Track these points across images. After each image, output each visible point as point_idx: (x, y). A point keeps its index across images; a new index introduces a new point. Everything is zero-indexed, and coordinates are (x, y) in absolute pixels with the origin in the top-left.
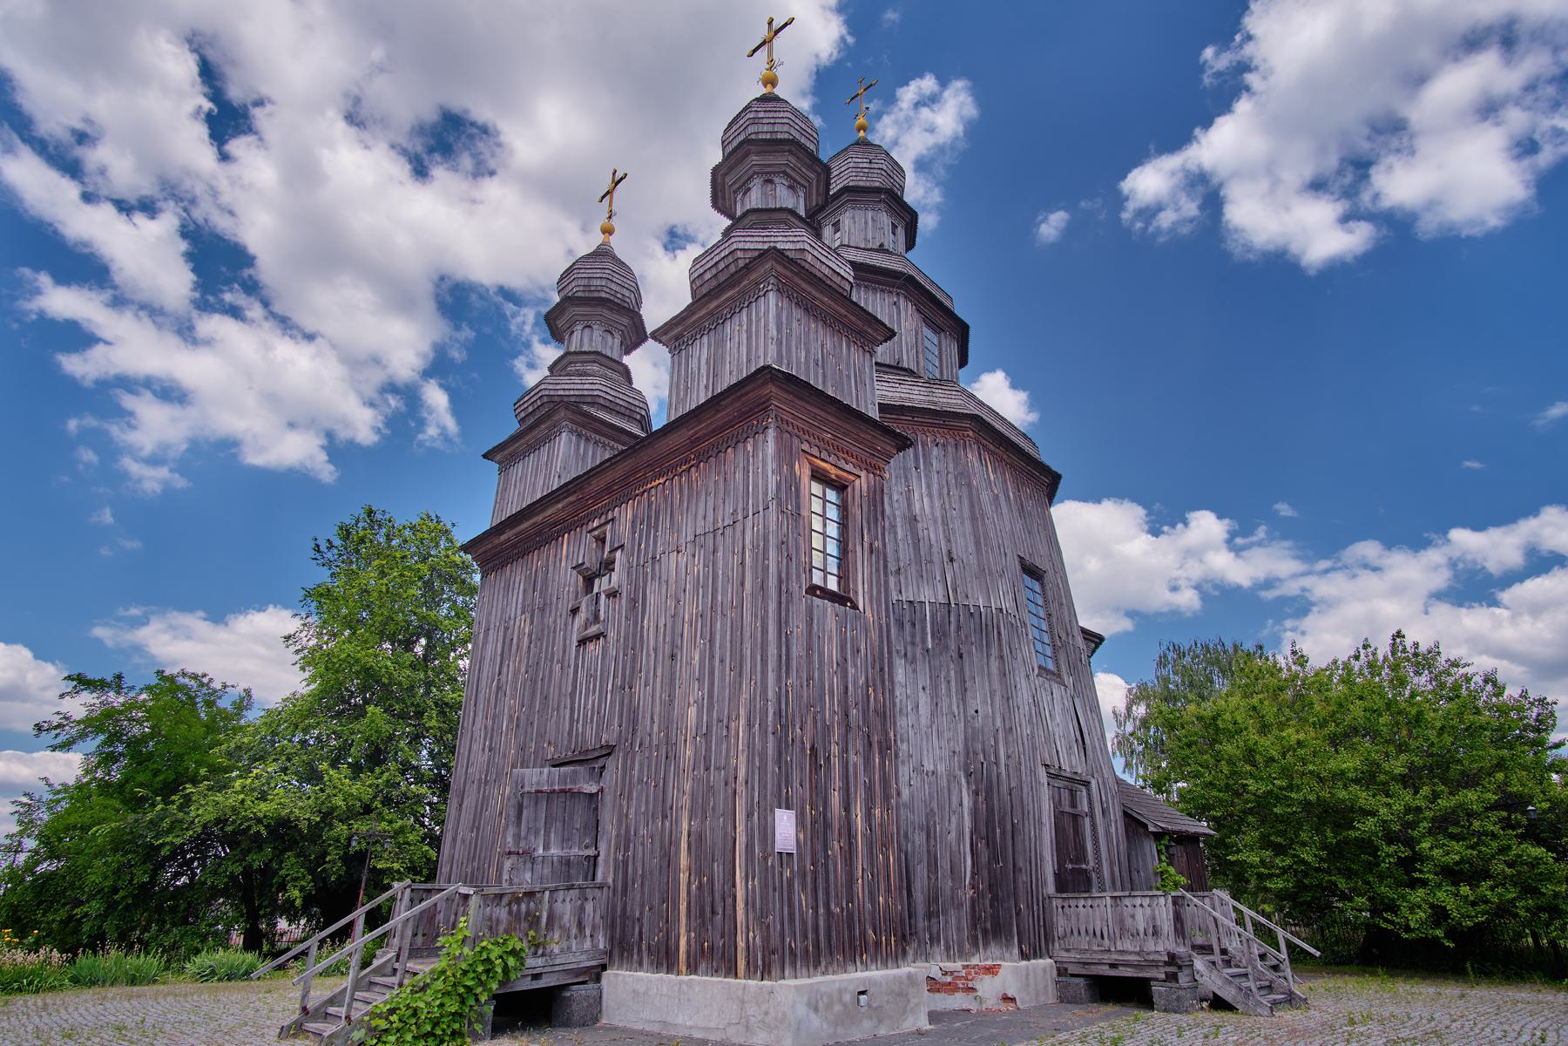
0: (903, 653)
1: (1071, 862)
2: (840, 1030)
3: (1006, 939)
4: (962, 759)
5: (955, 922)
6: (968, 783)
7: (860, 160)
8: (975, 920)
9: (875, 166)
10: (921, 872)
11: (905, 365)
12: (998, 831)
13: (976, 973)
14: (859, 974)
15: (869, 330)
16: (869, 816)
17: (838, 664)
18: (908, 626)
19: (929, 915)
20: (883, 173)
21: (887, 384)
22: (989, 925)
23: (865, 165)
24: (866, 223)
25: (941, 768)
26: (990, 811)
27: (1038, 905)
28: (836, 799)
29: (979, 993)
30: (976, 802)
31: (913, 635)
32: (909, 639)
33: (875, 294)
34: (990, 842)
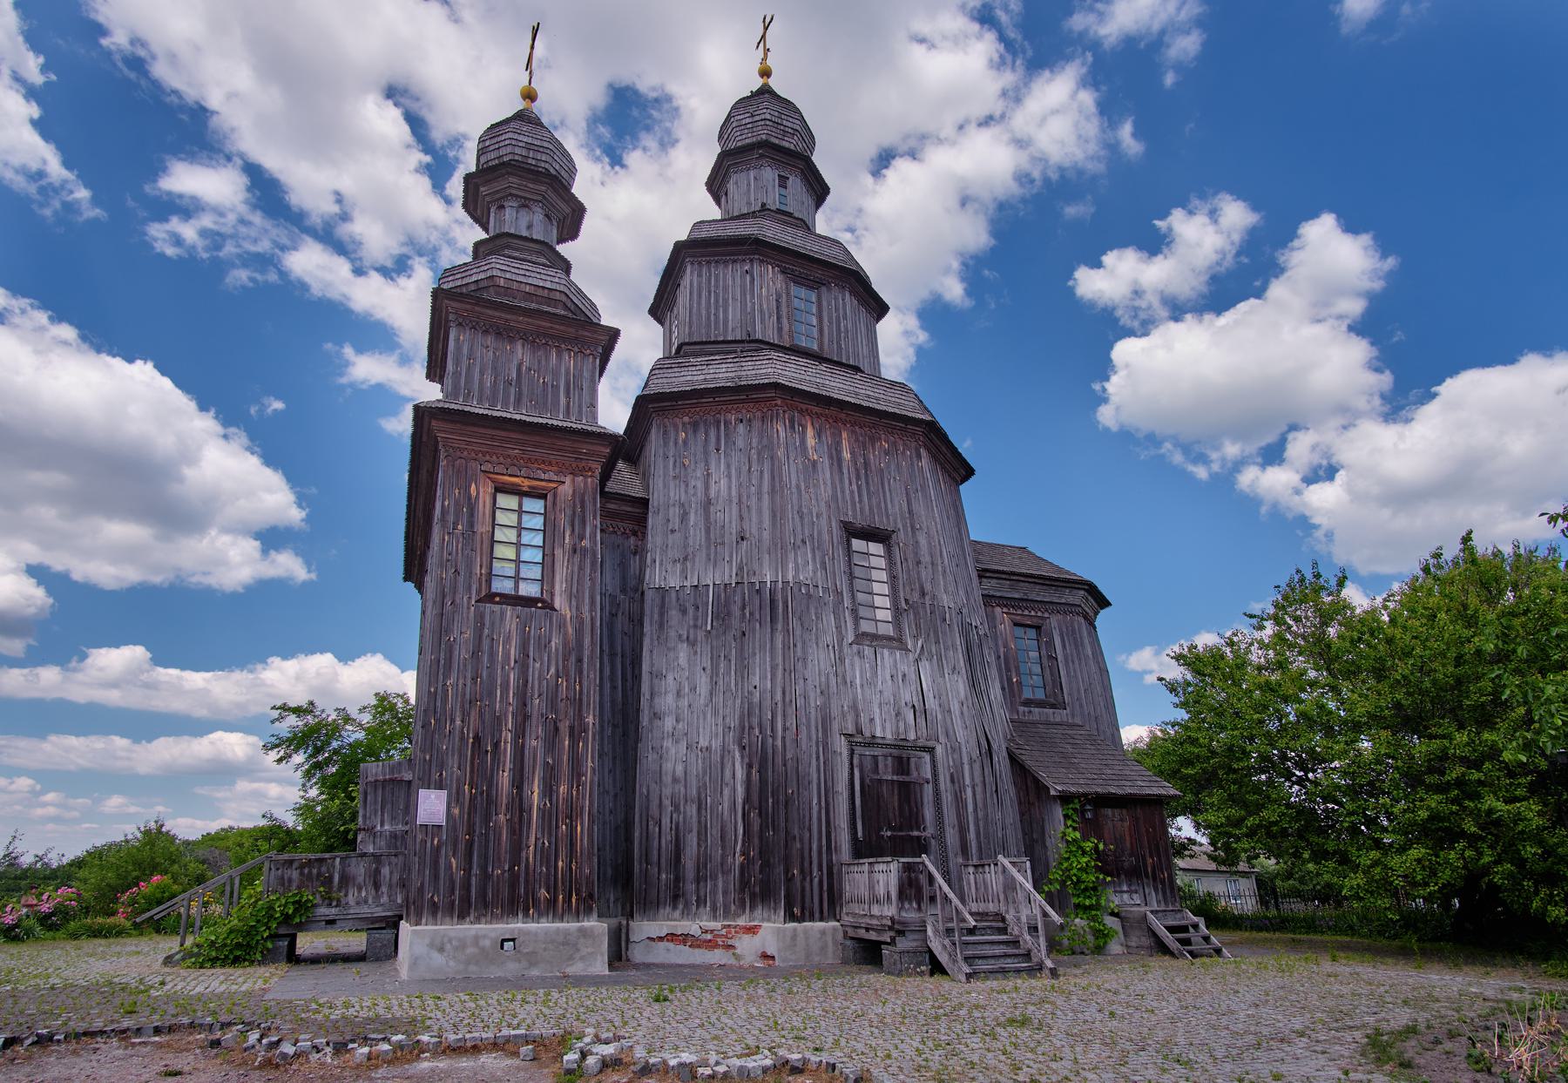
0: (685, 636)
1: (890, 828)
2: (472, 968)
3: (775, 903)
4: (737, 735)
5: (724, 886)
6: (742, 757)
7: (742, 117)
8: (744, 883)
9: (757, 118)
10: (692, 841)
11: (759, 336)
12: (770, 801)
13: (736, 932)
14: (520, 925)
15: (586, 334)
17: (516, 662)
18: (691, 611)
19: (698, 880)
20: (768, 123)
21: (694, 368)
22: (757, 889)
23: (748, 120)
24: (749, 185)
25: (716, 744)
26: (763, 781)
27: (820, 869)
28: (505, 779)
29: (738, 951)
30: (749, 775)
31: (696, 619)
32: (691, 623)
33: (726, 267)
34: (762, 813)
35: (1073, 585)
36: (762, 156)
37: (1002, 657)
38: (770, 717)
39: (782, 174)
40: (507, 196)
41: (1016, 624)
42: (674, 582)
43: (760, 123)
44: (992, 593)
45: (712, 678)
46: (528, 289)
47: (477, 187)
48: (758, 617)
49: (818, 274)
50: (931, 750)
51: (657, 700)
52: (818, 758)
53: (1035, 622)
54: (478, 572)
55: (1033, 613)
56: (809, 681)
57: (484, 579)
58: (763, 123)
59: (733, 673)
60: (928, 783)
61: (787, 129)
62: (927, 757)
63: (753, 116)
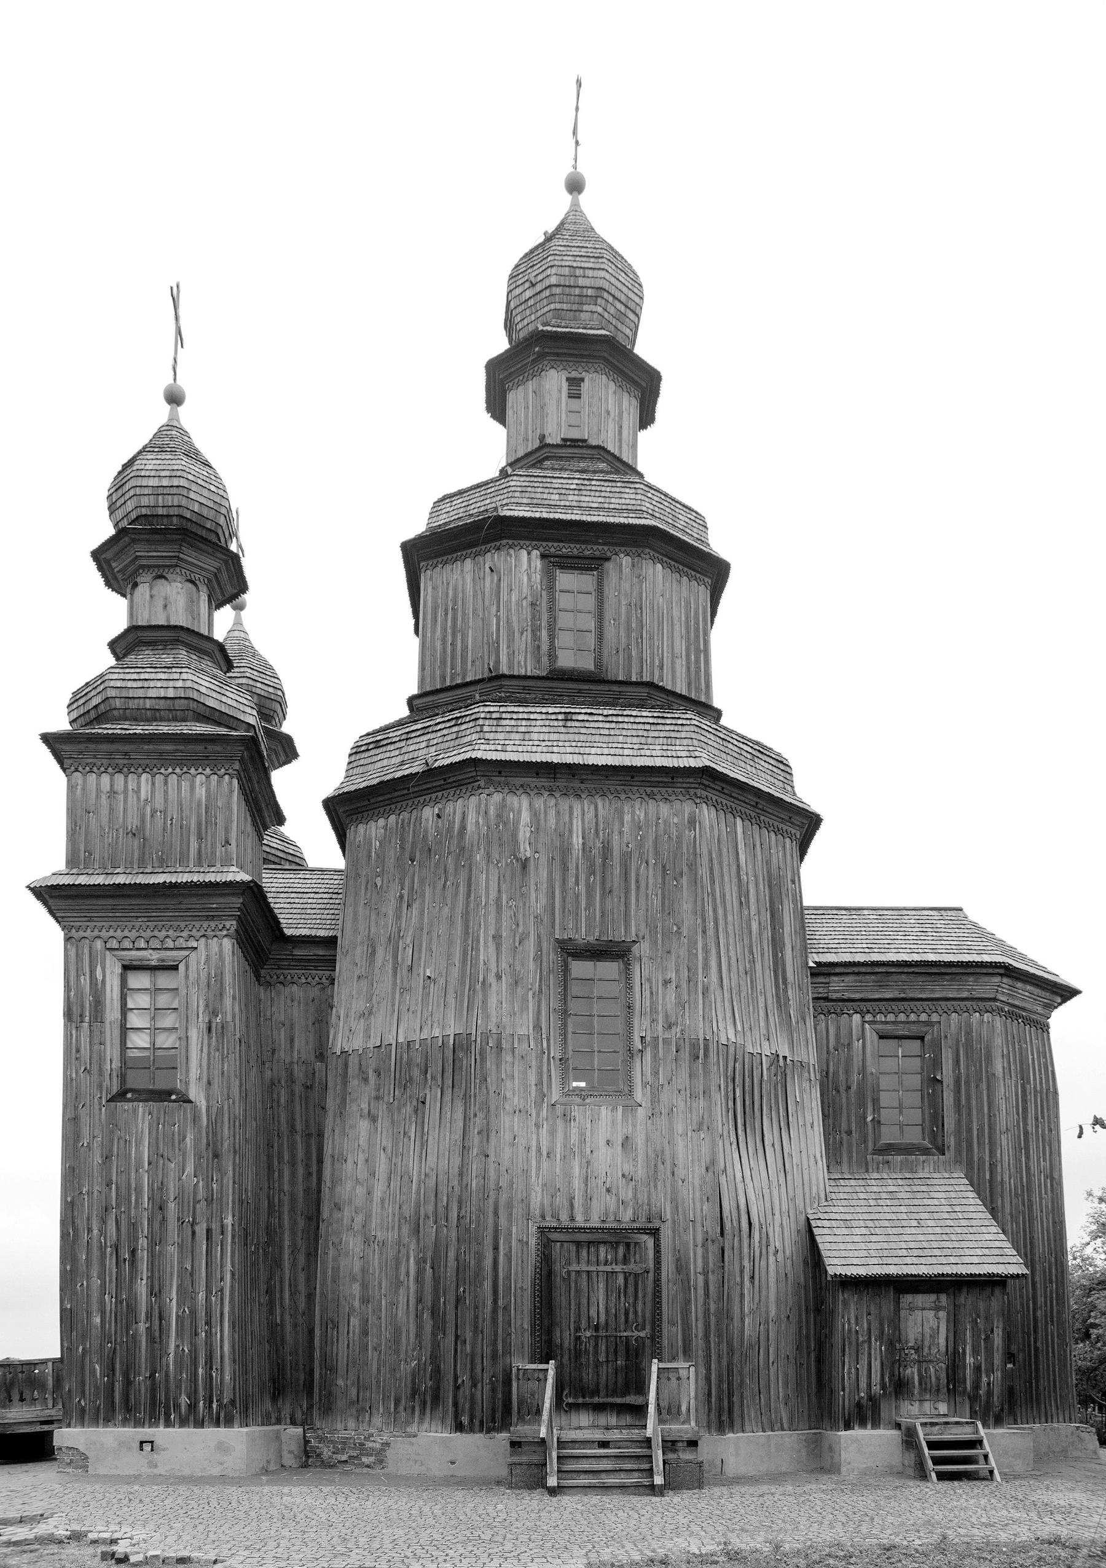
9: (539, 288)
16: (186, 1294)
18: (372, 1077)
21: (392, 747)
23: (528, 294)
35: (978, 970)
36: (541, 356)
37: (854, 1087)
38: (445, 1203)
40: (137, 570)
41: (881, 1037)
42: (357, 1043)
43: (544, 295)
44: (847, 995)
45: (390, 1160)
47: (108, 562)
48: (440, 1083)
49: (595, 550)
50: (655, 1233)
51: (338, 1189)
52: (496, 1248)
53: (915, 1030)
54: (109, 1068)
55: (913, 1017)
56: (492, 1158)
57: (115, 1074)
58: (547, 293)
59: (412, 1153)
60: (648, 1272)
62: (650, 1242)
63: (533, 285)
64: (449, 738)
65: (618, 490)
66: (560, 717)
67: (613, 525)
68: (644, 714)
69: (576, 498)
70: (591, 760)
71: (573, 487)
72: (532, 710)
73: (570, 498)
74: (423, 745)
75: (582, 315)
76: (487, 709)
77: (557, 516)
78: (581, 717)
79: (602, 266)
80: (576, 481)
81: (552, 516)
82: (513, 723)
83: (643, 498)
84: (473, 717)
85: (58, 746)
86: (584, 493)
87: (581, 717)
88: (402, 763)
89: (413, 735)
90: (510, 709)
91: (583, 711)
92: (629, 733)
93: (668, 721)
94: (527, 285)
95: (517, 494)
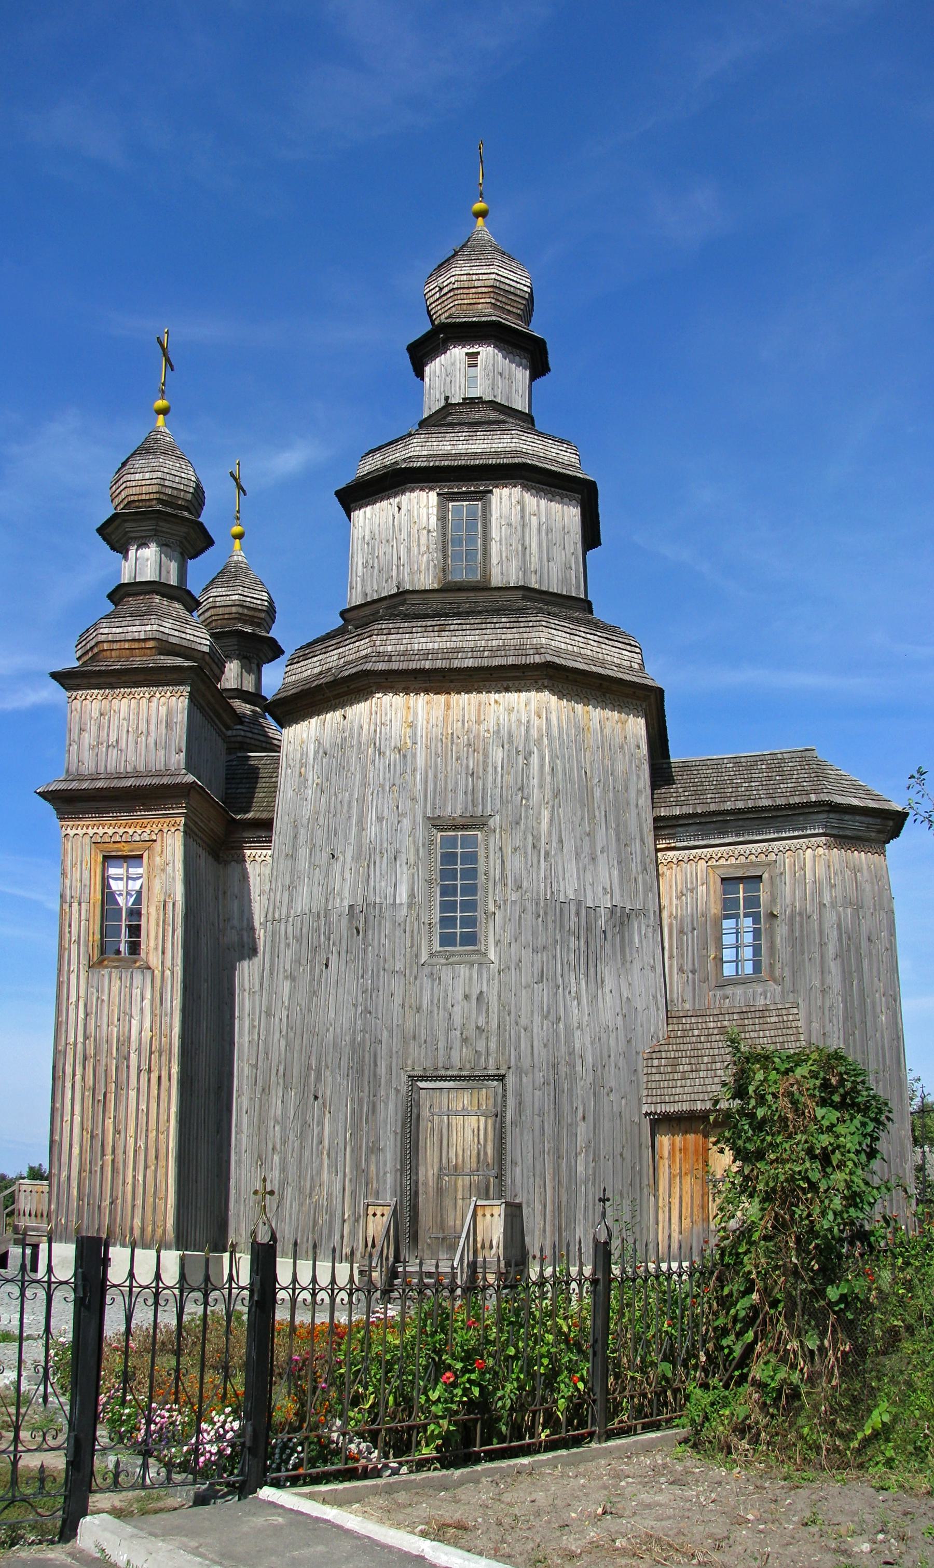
21: (315, 659)
39: (472, 350)
46: (127, 645)
58: (452, 294)
61: (480, 290)
64: (353, 651)
65: (498, 437)
66: (436, 628)
67: (491, 465)
68: (503, 620)
69: (464, 447)
70: (456, 664)
71: (462, 438)
72: (414, 624)
73: (460, 447)
74: (336, 657)
75: (480, 306)
76: (380, 627)
77: (446, 463)
78: (452, 627)
79: (492, 271)
80: (464, 434)
81: (443, 463)
82: (399, 636)
83: (517, 441)
84: (369, 634)
85: (62, 681)
86: (471, 442)
87: (452, 627)
88: (321, 673)
89: (330, 648)
90: (398, 625)
91: (455, 622)
92: (490, 637)
93: (522, 625)
94: (437, 289)
95: (418, 449)
